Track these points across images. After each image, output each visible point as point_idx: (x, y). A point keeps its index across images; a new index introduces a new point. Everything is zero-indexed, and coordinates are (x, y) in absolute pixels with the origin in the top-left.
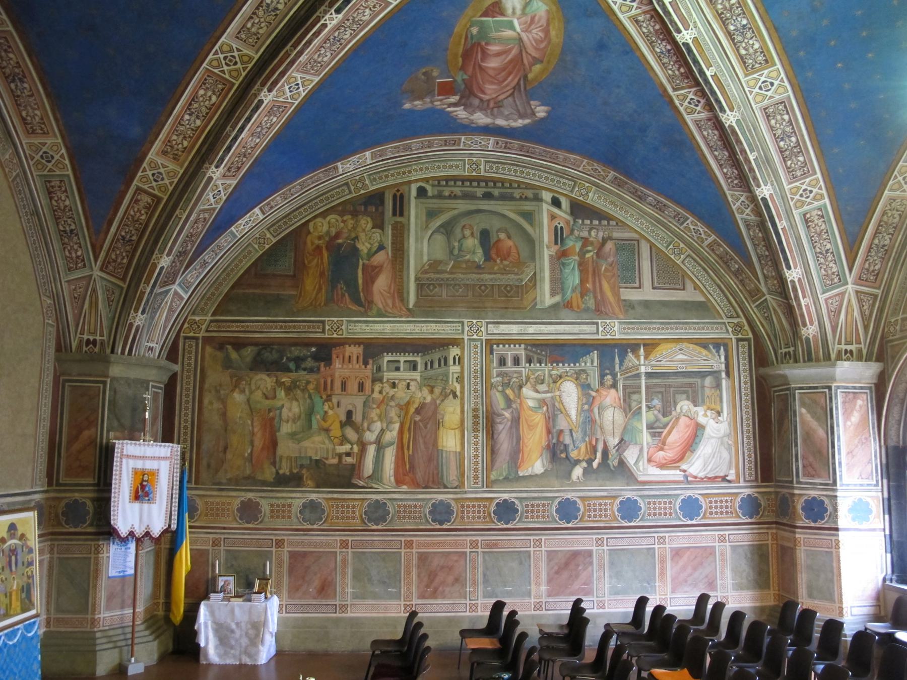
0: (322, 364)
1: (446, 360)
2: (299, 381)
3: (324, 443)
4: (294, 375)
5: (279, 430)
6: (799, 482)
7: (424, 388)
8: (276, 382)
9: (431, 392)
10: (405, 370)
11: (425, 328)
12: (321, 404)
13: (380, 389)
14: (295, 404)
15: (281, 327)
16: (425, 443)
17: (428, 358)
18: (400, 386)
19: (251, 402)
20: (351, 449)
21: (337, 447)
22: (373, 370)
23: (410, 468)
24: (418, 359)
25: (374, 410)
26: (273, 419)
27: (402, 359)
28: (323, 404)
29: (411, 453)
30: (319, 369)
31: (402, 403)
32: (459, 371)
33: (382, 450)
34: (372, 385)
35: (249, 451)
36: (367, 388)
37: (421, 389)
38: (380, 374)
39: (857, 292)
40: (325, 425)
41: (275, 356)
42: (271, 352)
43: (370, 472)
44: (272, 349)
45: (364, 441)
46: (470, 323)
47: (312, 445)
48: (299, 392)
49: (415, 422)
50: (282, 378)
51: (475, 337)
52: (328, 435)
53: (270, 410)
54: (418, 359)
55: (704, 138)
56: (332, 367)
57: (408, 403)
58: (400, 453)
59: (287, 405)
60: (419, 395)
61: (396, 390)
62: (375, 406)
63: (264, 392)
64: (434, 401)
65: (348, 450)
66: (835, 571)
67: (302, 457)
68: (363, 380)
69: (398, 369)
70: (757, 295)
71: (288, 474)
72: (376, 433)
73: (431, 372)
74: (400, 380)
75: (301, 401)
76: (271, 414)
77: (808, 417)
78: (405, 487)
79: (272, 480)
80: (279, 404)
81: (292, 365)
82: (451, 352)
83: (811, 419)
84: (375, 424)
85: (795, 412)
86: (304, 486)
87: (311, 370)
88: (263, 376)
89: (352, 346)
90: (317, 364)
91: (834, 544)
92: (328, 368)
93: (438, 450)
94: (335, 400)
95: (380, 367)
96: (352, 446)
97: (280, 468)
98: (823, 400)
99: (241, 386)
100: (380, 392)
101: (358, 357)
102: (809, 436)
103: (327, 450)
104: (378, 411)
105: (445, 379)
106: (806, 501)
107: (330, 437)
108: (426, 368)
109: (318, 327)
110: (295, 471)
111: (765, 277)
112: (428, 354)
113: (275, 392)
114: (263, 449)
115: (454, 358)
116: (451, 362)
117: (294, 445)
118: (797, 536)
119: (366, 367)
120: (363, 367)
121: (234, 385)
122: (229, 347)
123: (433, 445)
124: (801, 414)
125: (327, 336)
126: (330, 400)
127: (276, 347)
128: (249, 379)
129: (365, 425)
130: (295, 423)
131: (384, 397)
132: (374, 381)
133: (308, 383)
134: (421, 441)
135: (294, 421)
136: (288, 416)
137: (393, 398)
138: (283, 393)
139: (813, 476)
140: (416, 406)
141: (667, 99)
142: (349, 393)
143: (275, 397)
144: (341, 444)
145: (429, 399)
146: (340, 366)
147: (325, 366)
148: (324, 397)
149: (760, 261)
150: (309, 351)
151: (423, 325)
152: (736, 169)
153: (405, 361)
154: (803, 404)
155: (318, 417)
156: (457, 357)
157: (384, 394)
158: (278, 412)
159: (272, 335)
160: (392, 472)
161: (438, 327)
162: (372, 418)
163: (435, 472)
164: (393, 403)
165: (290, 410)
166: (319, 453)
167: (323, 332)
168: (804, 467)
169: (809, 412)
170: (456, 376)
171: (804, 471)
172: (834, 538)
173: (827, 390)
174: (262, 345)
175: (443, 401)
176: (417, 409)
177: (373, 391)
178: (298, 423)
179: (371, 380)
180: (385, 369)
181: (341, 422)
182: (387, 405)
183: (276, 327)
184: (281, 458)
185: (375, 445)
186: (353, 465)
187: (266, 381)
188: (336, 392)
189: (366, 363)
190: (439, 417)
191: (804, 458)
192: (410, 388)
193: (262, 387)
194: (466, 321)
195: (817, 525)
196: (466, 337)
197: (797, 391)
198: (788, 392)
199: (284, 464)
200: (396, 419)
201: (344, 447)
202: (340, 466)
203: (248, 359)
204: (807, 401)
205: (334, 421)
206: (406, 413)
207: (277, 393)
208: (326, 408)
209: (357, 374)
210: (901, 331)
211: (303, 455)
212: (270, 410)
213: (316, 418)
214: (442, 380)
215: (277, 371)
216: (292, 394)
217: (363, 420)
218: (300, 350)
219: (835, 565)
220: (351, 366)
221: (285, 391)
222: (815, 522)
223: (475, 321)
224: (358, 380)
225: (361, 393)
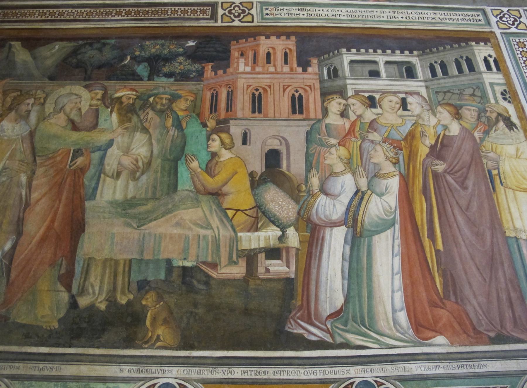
0: (209, 67)
1: (469, 61)
2: (156, 95)
3: (208, 226)
4: (143, 86)
5: (93, 196)
7: (439, 108)
8: (103, 98)
9: (457, 115)
10: (390, 77)
11: (417, 16)
12: (203, 138)
13: (342, 107)
14: (139, 137)
15: (128, 13)
16: (471, 222)
17: (435, 58)
18: (386, 103)
19: (37, 138)
20: (281, 239)
21: (240, 234)
22: (321, 75)
23: (445, 285)
24: (414, 60)
25: (333, 150)
26: (83, 170)
27: (381, 59)
28: (208, 139)
29: (440, 246)
30: (200, 74)
31: (398, 137)
32: (503, 81)
33: (364, 243)
34: (323, 102)
35: (8, 246)
36: (311, 106)
37: (433, 110)
38: (338, 83)
40: (211, 183)
41: (108, 54)
42: (100, 50)
43: (339, 301)
44: (104, 45)
45: (314, 218)
46: (496, 13)
47: (176, 231)
48: (151, 114)
49: (436, 175)
50: (116, 92)
51: (513, 30)
52: (219, 205)
53: (78, 153)
54: (414, 60)
56: (230, 70)
57: (411, 136)
58: (413, 247)
59: (120, 140)
60: (433, 121)
61: (378, 110)
62: (333, 141)
63: (72, 116)
64: (467, 133)
65: (273, 243)
67: (148, 262)
68: (301, 91)
69: (375, 74)
71: (103, 307)
72: (345, 199)
73: (446, 82)
74: (384, 93)
75: (155, 134)
76: (80, 160)
78: (440, 339)
79: (56, 325)
80: (103, 138)
81: (142, 69)
82: (476, 52)
84: (340, 180)
86: (146, 343)
87: (184, 77)
88: (79, 89)
89: (273, 38)
90: (197, 66)
92: (220, 72)
93: (506, 239)
94: (236, 130)
95: (336, 71)
96: (283, 229)
97: (82, 292)
99: (23, 108)
100: (343, 114)
101: (286, 54)
103: (217, 243)
104: (343, 151)
105: (478, 93)
107: (224, 211)
108: (434, 73)
109: (204, 12)
110: (123, 300)
112: (431, 52)
113: (97, 118)
114: (43, 240)
115: (486, 60)
116: (483, 67)
117: (129, 230)
119: (305, 70)
120: (300, 70)
121: (7, 106)
122: (17, 45)
123: (493, 228)
125: (219, 23)
126: (227, 131)
127: (113, 41)
128: (43, 95)
129: (315, 181)
130: (135, 179)
131: (353, 125)
132: (325, 94)
133: (174, 98)
134: (460, 219)
135: (134, 175)
136: (119, 163)
137: (373, 125)
138: (114, 116)
140: (430, 141)
142: (271, 115)
143: (95, 126)
144: (254, 227)
145: (455, 129)
146: (248, 69)
147: (215, 69)
148: (211, 124)
150: (181, 46)
151: (409, 11)
153: (387, 63)
155: (195, 164)
156: (491, 60)
157: (353, 117)
158: (96, 156)
159: (108, 25)
160: (399, 298)
161: (440, 15)
162: (330, 166)
163: (513, 295)
164: (375, 136)
165: (127, 151)
166: (193, 251)
167: (214, 17)
170: (499, 89)
174: (83, 39)
175: (487, 133)
176: (433, 148)
177: (325, 112)
178: (144, 178)
179: (318, 93)
180: (348, 74)
181: (252, 175)
182: (363, 139)
183: (118, 13)
184: (89, 263)
185: (343, 229)
186: (289, 282)
187: (79, 96)
188: (240, 115)
189: (304, 64)
190: (488, 164)
192: (409, 107)
193: (67, 109)
194: (488, 9)
196: (498, 32)
199: (94, 278)
200: (388, 168)
201: (262, 234)
202: (252, 284)
203: (49, 62)
205: (236, 173)
206: (412, 155)
207: (101, 120)
208: (215, 145)
209: (287, 82)
211: (147, 256)
212: (78, 153)
213: (189, 168)
214: (473, 95)
215: (109, 79)
216: (135, 119)
217: (308, 170)
218: (163, 45)
220: (272, 69)
221: (119, 114)
223: (505, 9)
224: (290, 91)
225: (298, 116)
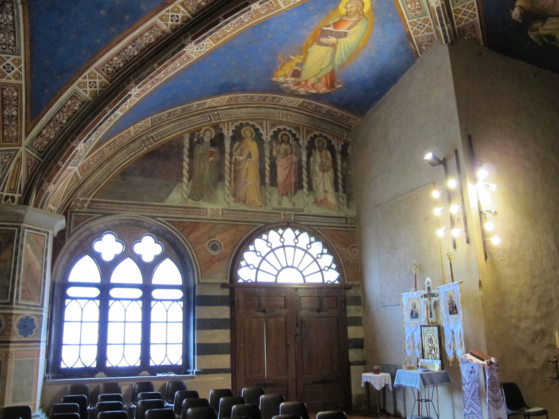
6: (17, 304)
39: (75, 174)
55: (141, 35)
66: (35, 375)
70: (11, 142)
77: (31, 252)
83: (33, 255)
85: (22, 245)
91: (36, 353)
98: (42, 241)
102: (29, 267)
106: (21, 319)
111: (40, 134)
118: (11, 349)
124: (26, 249)
139: (28, 299)
141: (169, 2)
149: (50, 122)
152: (124, 65)
154: (29, 242)
168: (23, 291)
169: (32, 248)
171: (22, 294)
172: (37, 349)
173: (46, 235)
191: (24, 284)
195: (27, 339)
197: (26, 230)
198: (16, 229)
204: (32, 239)
210: (89, 207)
219: (35, 370)
222: (25, 336)
